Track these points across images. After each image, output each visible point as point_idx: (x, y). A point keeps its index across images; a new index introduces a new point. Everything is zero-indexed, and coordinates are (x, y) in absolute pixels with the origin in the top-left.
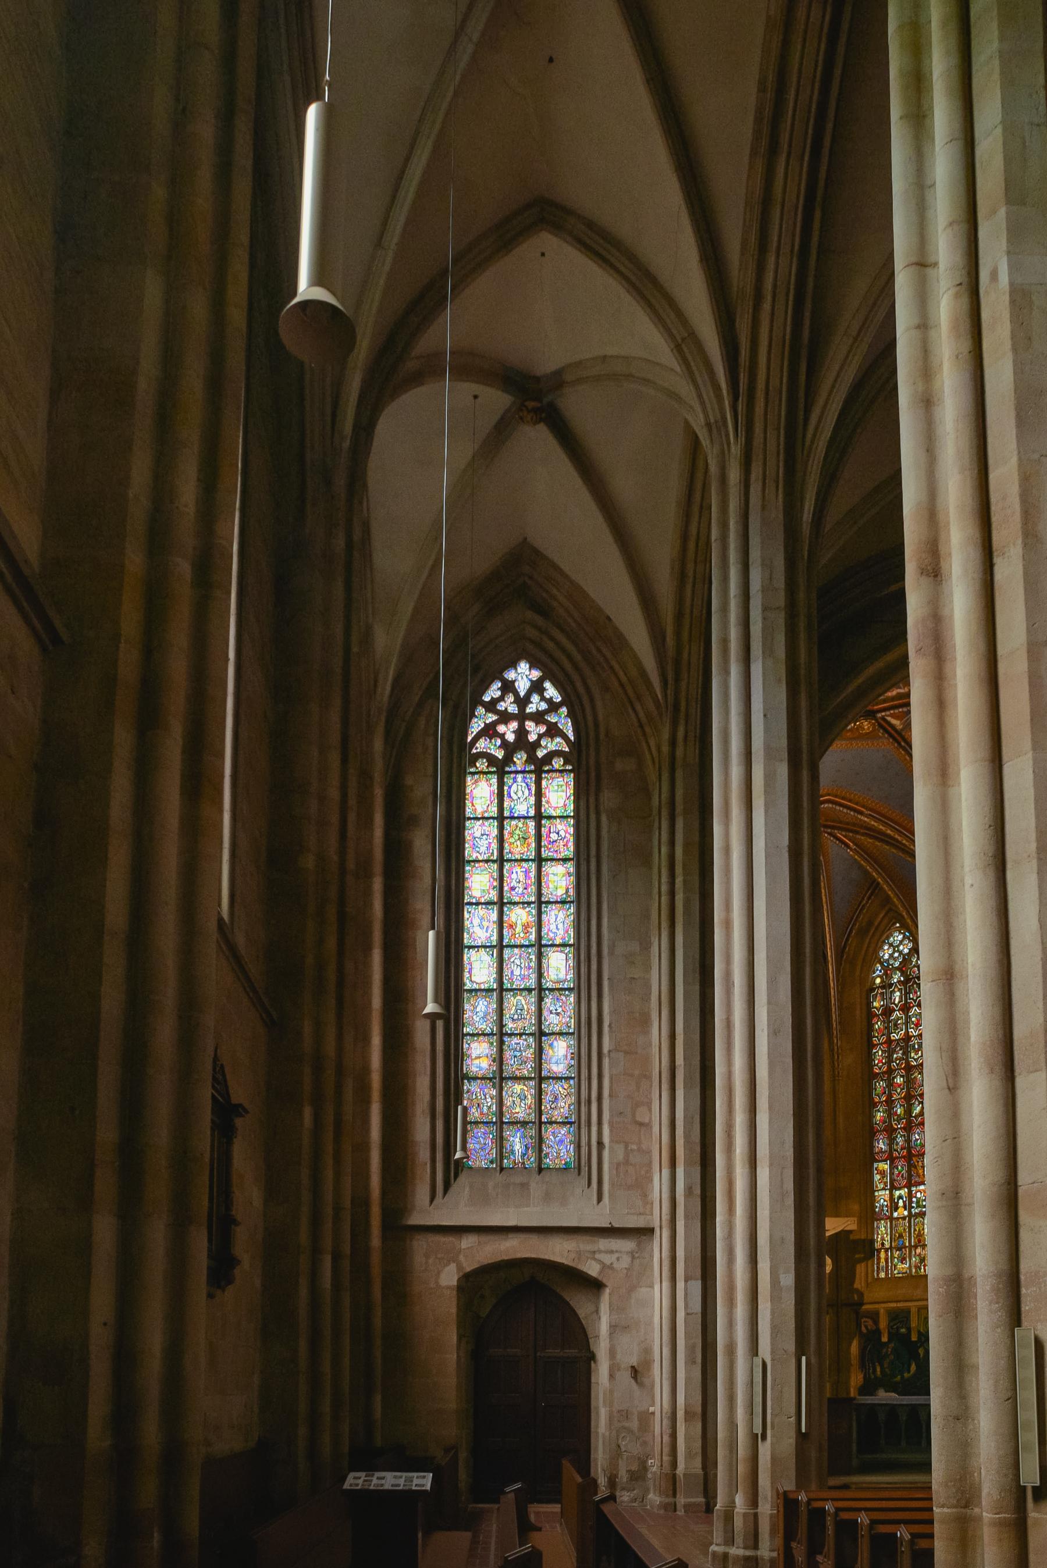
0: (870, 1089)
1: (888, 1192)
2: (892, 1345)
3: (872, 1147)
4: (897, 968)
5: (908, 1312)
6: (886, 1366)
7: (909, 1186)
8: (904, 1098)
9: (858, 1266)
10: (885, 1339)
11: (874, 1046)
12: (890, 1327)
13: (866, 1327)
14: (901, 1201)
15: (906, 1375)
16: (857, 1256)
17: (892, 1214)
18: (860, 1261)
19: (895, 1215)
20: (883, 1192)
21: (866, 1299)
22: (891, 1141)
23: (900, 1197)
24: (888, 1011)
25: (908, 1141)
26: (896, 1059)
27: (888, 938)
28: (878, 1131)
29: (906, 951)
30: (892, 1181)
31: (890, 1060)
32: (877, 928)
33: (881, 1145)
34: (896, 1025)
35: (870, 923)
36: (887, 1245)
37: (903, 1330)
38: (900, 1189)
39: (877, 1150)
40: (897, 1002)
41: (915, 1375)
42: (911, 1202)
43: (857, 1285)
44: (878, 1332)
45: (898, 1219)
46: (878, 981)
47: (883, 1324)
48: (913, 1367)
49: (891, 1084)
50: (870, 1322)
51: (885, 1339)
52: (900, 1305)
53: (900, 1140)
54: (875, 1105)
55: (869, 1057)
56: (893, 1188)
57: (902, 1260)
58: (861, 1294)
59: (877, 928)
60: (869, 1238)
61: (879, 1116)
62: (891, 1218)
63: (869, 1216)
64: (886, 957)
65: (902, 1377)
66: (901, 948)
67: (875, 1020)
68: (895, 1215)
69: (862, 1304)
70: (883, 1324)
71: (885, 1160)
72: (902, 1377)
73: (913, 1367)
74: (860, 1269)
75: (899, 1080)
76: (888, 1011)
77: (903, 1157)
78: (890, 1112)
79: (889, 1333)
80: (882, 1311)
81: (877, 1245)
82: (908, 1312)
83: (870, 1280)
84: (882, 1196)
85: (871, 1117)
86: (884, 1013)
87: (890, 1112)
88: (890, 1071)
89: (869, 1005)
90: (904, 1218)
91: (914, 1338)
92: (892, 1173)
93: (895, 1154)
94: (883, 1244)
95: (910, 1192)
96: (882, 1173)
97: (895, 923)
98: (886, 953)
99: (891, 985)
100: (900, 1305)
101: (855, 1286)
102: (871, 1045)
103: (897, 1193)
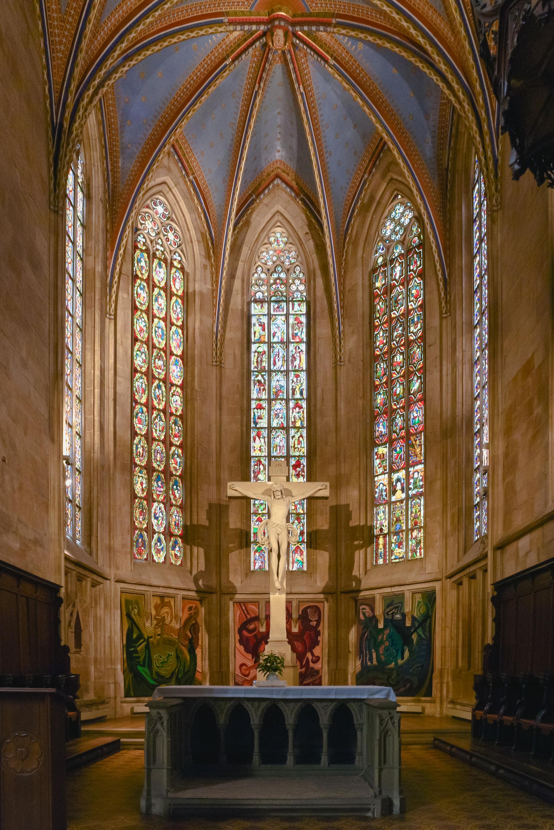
0: (373, 371)
1: (387, 475)
2: (387, 632)
3: (373, 431)
4: (399, 242)
5: (401, 596)
6: (381, 652)
7: (406, 467)
8: (403, 376)
9: (357, 553)
10: (381, 626)
11: (376, 327)
12: (385, 613)
13: (364, 614)
14: (399, 484)
15: (400, 662)
16: (356, 543)
17: (390, 498)
18: (359, 547)
19: (393, 499)
20: (382, 477)
21: (362, 587)
22: (392, 421)
23: (398, 480)
24: (388, 289)
25: (407, 420)
26: (396, 337)
27: (390, 213)
28: (378, 415)
29: (407, 221)
30: (391, 463)
31: (390, 338)
32: (379, 202)
33: (381, 428)
34: (396, 302)
35: (372, 198)
36: (386, 531)
37: (398, 616)
38: (398, 471)
39: (377, 434)
40: (397, 278)
41: (408, 660)
42: (408, 483)
43: (355, 573)
44: (373, 619)
45: (395, 502)
46: (380, 260)
47: (379, 611)
48: (407, 654)
49: (391, 364)
50: (368, 609)
51: (381, 626)
52: (395, 589)
53: (399, 421)
54: (376, 388)
55: (372, 338)
56: (392, 471)
57: (399, 545)
58: (359, 581)
59: (379, 202)
60: (369, 524)
61: (380, 399)
62: (389, 503)
63: (370, 502)
64: (388, 233)
65: (396, 664)
66: (402, 220)
67: (377, 300)
68: (393, 499)
69: (359, 591)
70: (379, 611)
71: (385, 444)
72: (396, 664)
73: (407, 654)
74: (359, 555)
75: (399, 358)
76: (388, 289)
77: (402, 438)
78: (390, 394)
79: (386, 621)
80: (378, 597)
81: (376, 532)
82: (401, 596)
83: (369, 567)
84: (382, 480)
85: (372, 400)
86: (385, 292)
87: (390, 394)
88: (391, 350)
89: (371, 285)
90: (401, 501)
91: (408, 624)
92: (391, 456)
93: (394, 436)
94: (381, 530)
95: (408, 473)
96: (382, 457)
97: (396, 196)
98: (388, 229)
99: (392, 261)
100: (395, 589)
101: (354, 574)
102: (372, 328)
103: (395, 476)
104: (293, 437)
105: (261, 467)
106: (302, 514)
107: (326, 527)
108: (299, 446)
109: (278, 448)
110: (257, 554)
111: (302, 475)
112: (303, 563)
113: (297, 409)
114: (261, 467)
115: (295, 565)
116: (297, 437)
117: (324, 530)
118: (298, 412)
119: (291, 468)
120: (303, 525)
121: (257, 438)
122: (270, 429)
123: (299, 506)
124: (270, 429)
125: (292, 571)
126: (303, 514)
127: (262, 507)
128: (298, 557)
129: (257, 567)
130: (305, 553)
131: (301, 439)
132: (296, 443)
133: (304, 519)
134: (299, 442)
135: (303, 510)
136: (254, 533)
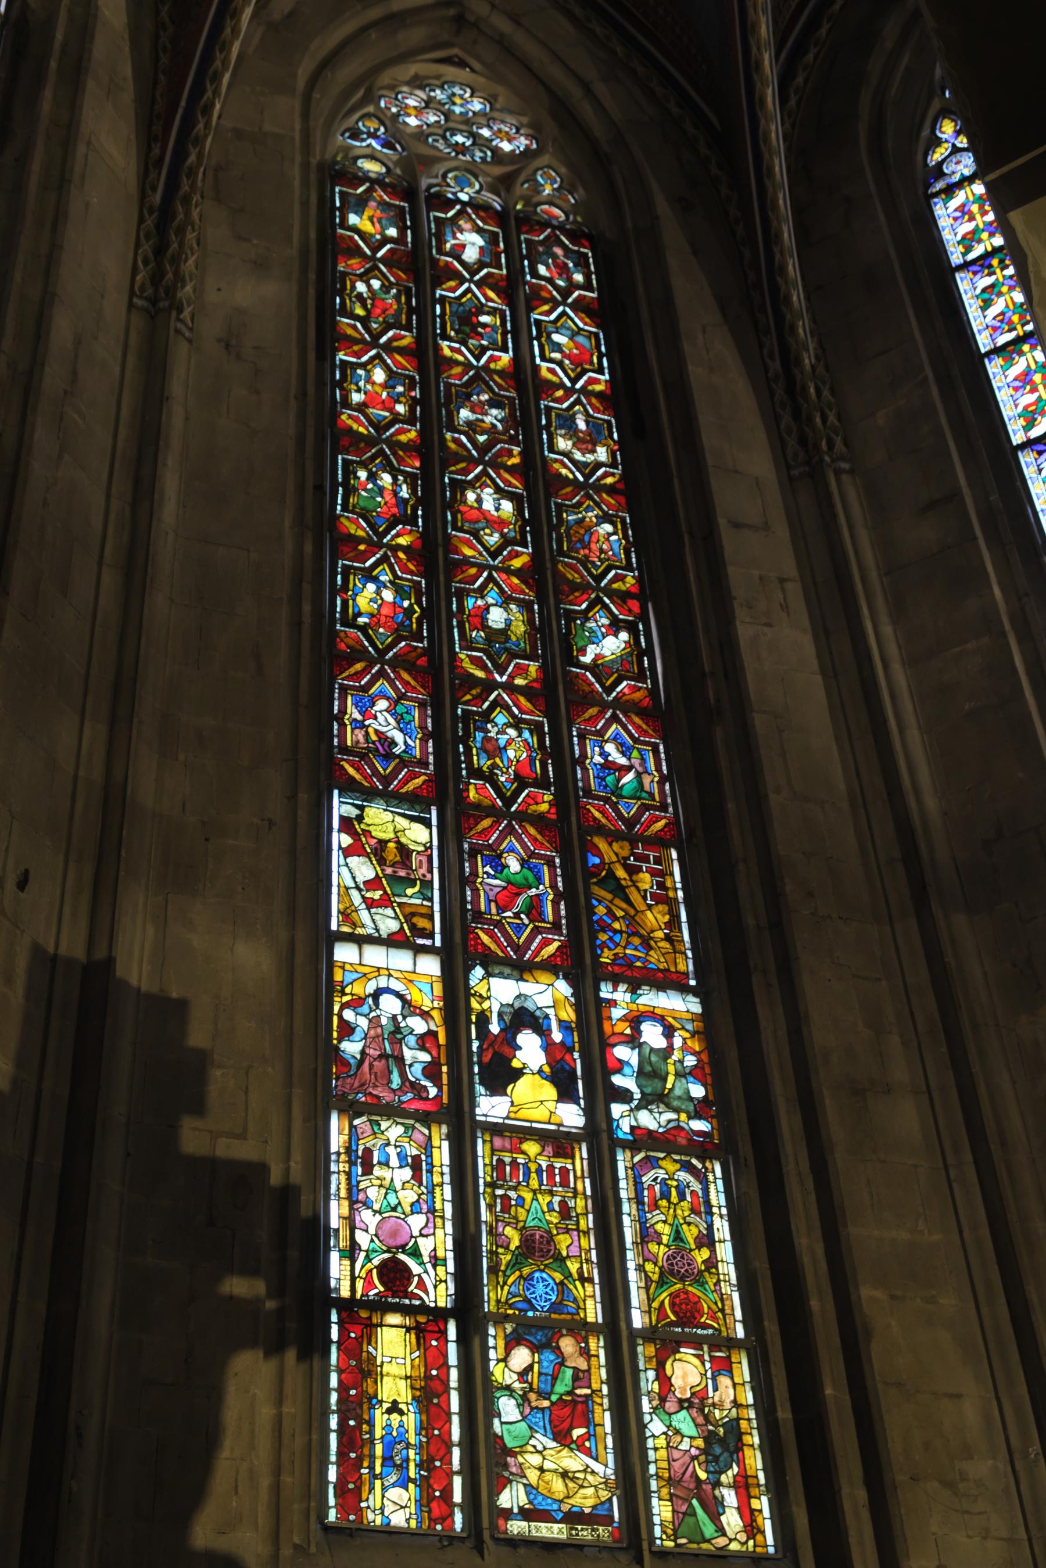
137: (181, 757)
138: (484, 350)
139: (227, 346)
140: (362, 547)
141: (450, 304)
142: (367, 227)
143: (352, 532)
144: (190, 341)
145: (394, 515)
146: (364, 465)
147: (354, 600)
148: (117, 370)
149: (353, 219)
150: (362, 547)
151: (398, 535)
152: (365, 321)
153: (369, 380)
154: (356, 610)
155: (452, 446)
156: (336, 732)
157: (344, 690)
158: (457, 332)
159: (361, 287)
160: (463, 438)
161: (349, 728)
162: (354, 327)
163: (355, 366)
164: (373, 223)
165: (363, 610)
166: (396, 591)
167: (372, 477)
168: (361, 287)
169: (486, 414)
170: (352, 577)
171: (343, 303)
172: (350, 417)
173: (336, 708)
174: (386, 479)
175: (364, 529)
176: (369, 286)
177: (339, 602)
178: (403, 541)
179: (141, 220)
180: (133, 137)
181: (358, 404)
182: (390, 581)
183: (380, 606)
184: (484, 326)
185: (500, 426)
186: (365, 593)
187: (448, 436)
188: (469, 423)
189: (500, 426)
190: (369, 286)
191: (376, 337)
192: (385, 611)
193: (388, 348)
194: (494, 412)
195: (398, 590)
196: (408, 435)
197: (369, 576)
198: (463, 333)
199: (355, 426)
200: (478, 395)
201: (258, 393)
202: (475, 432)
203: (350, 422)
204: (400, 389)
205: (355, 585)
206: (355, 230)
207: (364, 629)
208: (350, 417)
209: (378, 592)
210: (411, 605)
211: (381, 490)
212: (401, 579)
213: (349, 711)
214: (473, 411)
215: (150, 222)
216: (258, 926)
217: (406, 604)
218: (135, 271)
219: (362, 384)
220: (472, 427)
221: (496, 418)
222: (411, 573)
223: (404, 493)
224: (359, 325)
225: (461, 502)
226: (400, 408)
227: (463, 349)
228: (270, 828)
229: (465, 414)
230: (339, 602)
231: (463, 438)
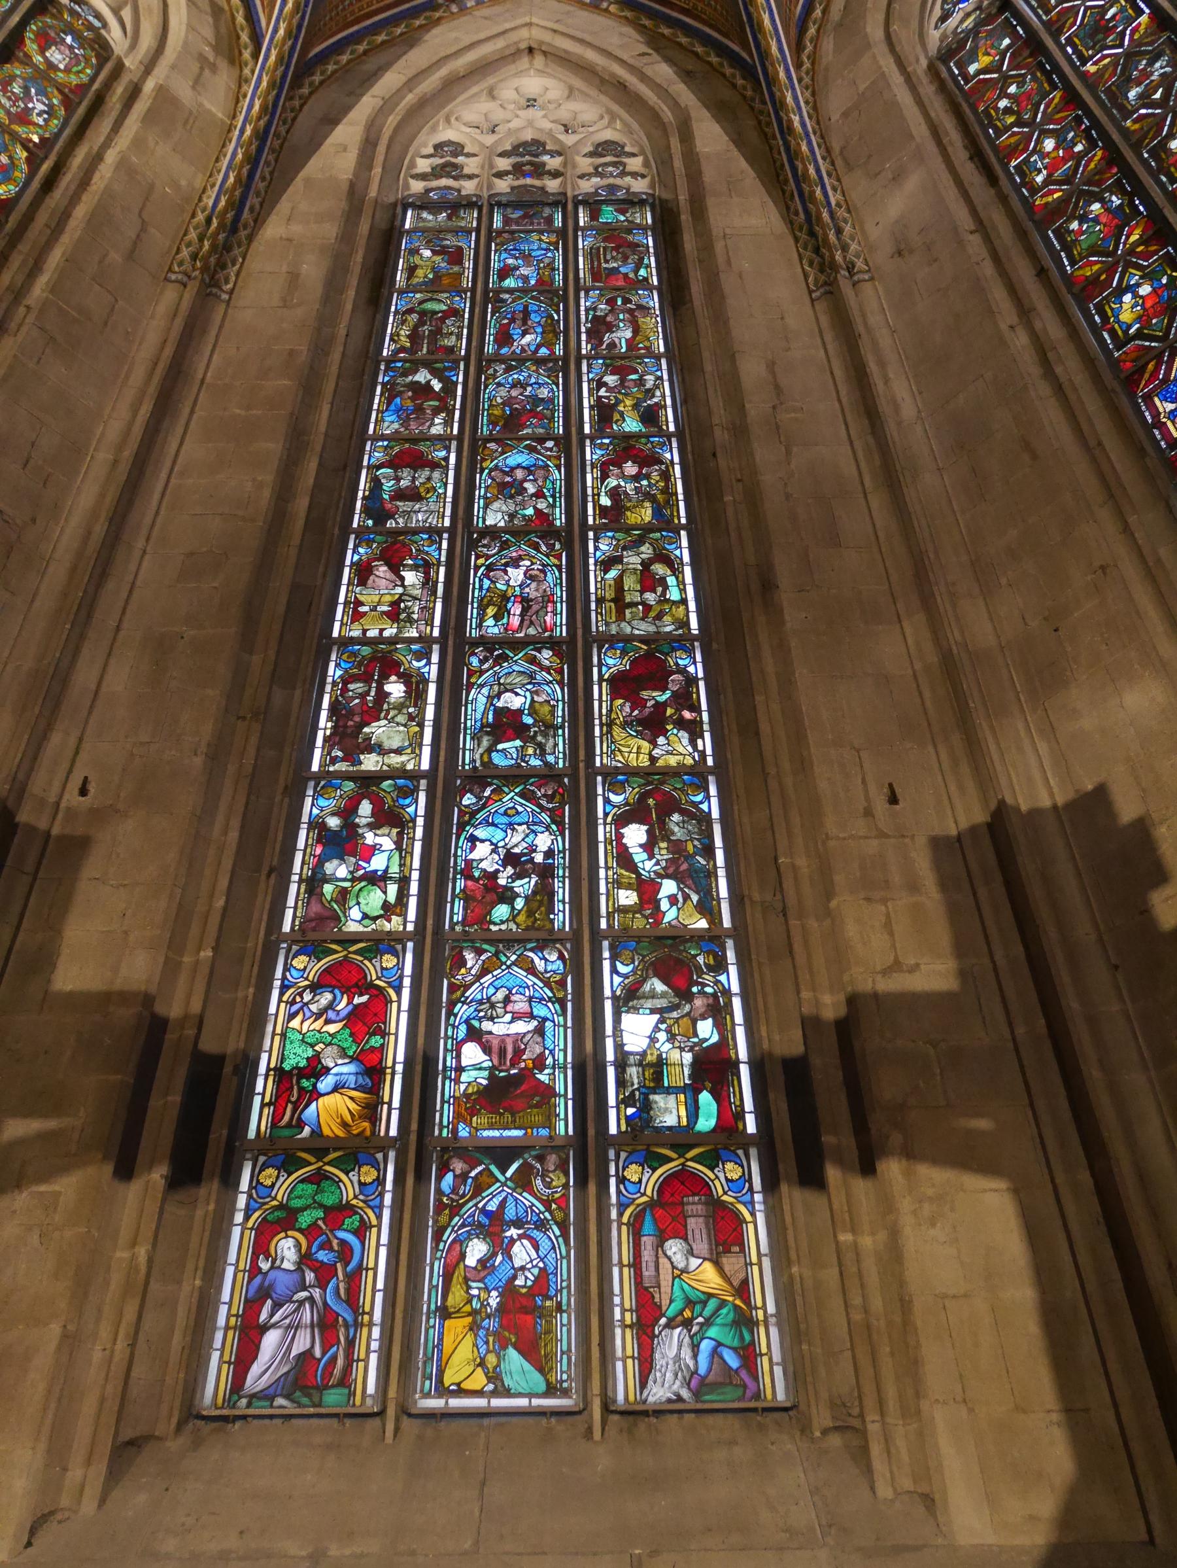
104: (606, 564)
105: (395, 689)
106: (698, 937)
107: (933, 973)
108: (650, 597)
109: (517, 609)
110: (287, 1248)
111: (681, 724)
112: (744, 1321)
113: (630, 468)
114: (395, 689)
115: (671, 1346)
116: (633, 560)
117: (912, 1002)
118: (636, 478)
119: (599, 692)
120: (718, 1011)
121: (382, 570)
122: (467, 535)
123: (669, 887)
124: (467, 535)
125: (637, 1414)
126: (712, 939)
127: (373, 899)
128: (689, 1267)
129: (259, 1376)
130: (757, 1232)
131: (660, 569)
132: (630, 582)
133: (720, 966)
134: (649, 581)
135: (707, 908)
136: (282, 1076)
137: (1004, 581)
138: (1122, 34)
139: (900, 253)
140: (1103, 277)
141: (1076, 36)
142: (985, 60)
143: (1088, 274)
144: (872, 279)
145: (1117, 226)
146: (1069, 220)
147: (1118, 322)
148: (822, 352)
149: (972, 69)
150: (1103, 277)
151: (1128, 237)
152: (1019, 123)
153: (1044, 156)
154: (1124, 327)
155: (1137, 126)
156: (1159, 437)
157: (1148, 399)
158: (1092, 48)
159: (1003, 103)
160: (1143, 111)
161: (1169, 424)
162: (1014, 134)
163: (1027, 160)
164: (988, 54)
165: (1129, 322)
166: (1151, 280)
167: (1083, 219)
168: (1003, 103)
169: (1152, 73)
170: (1107, 308)
171: (996, 128)
172: (1042, 197)
173: (1149, 418)
174: (1096, 207)
175: (1096, 262)
176: (1009, 96)
177: (1106, 335)
178: (1133, 238)
179: (796, 240)
180: (767, 199)
181: (1045, 181)
182: (1141, 277)
183: (1143, 305)
184: (1114, 16)
185: (1168, 69)
186: (1125, 306)
187: (1129, 123)
188: (1140, 97)
189: (1168, 69)
190: (1009, 96)
191: (1031, 123)
192: (1149, 304)
193: (1048, 118)
194: (1158, 65)
195: (1148, 276)
196: (1096, 158)
197: (1120, 291)
198: (1099, 41)
199: (1050, 199)
200: (1136, 69)
201: (936, 260)
202: (1149, 96)
203: (1045, 200)
204: (1071, 134)
205: (1112, 309)
206: (979, 72)
207: (1139, 335)
208: (1042, 197)
209: (1136, 295)
210: (1170, 277)
211: (1096, 220)
212: (1148, 266)
213: (1161, 410)
214: (1138, 85)
215: (803, 236)
216: (1136, 666)
217: (1164, 281)
218: (806, 276)
219: (1039, 165)
220: (1145, 99)
221: (1162, 68)
222: (1156, 252)
223: (1116, 201)
224: (1015, 129)
225: (1168, 157)
226: (1079, 148)
227: (1105, 52)
228: (1105, 573)
229: (1132, 94)
230: (1106, 335)
231: (1143, 111)
